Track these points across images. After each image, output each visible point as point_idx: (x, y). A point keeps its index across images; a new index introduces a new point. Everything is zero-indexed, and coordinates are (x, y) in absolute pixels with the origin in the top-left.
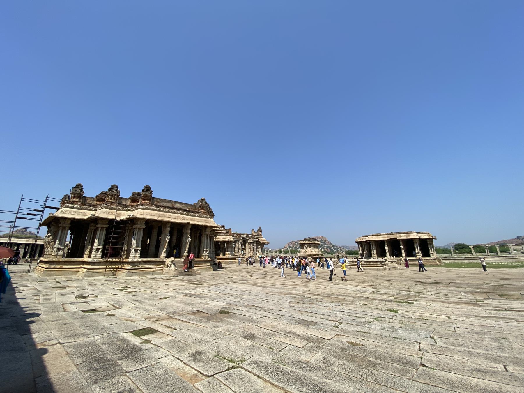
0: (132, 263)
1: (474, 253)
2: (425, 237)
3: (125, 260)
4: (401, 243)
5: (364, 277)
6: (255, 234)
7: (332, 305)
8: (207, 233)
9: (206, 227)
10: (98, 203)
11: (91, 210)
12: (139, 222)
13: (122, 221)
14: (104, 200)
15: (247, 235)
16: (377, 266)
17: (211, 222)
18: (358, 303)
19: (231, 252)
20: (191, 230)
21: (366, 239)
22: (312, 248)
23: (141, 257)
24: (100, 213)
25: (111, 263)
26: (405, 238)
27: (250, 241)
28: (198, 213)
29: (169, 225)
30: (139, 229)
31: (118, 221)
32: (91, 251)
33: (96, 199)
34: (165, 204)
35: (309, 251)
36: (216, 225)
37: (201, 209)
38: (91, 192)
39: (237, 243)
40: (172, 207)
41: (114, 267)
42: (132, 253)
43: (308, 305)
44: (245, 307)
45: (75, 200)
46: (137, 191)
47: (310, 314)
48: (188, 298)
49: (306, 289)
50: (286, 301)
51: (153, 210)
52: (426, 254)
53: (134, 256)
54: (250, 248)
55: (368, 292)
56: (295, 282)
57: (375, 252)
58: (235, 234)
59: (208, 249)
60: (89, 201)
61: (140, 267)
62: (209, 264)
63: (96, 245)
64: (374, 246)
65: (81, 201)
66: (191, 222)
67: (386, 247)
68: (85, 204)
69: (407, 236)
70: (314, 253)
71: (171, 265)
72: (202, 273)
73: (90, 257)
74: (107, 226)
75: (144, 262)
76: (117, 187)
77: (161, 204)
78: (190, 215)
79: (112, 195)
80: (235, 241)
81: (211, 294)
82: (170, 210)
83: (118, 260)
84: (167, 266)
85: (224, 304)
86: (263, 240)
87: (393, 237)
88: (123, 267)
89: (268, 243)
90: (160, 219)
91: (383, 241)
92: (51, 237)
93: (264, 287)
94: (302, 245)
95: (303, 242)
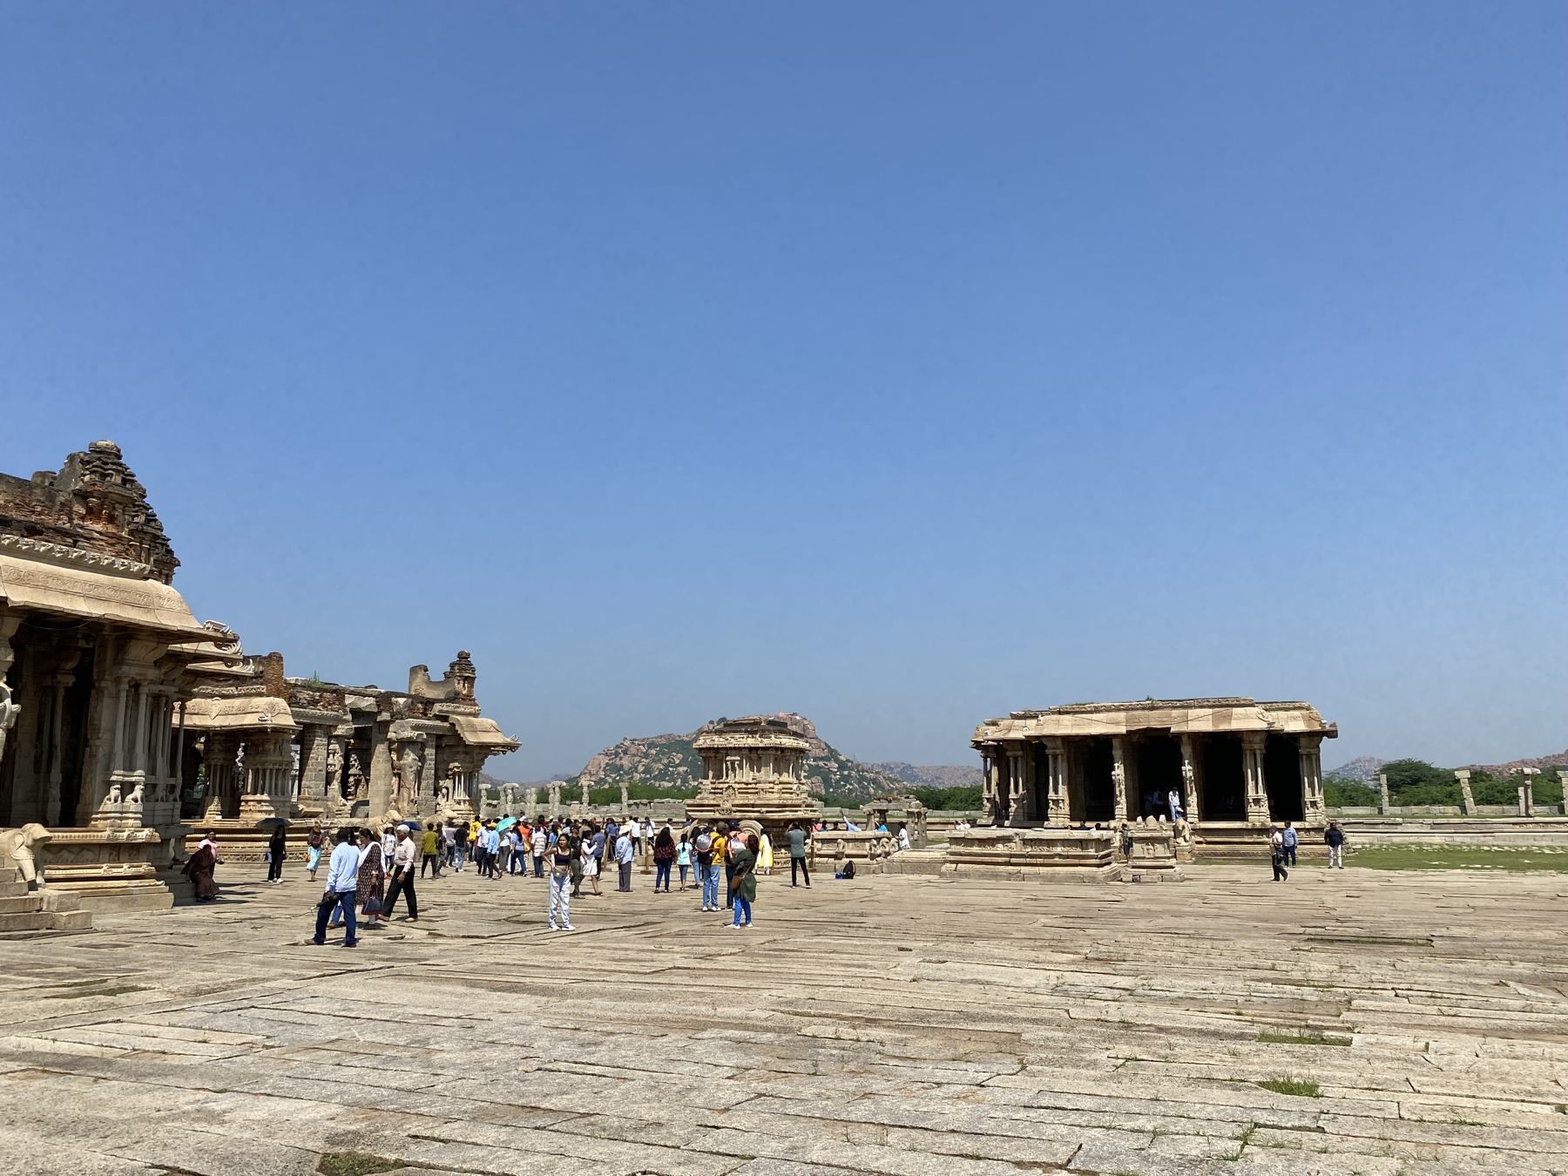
1: (1469, 802)
2: (1293, 724)
4: (1186, 750)
5: (1044, 920)
6: (430, 694)
7: (973, 1072)
8: (130, 671)
9: (126, 633)
15: (385, 700)
16: (1080, 861)
17: (164, 605)
18: (1102, 1056)
19: (279, 793)
21: (1029, 729)
22: (767, 774)
26: (1206, 726)
27: (403, 730)
28: (72, 537)
35: (746, 789)
36: (193, 625)
37: (92, 513)
39: (319, 742)
43: (851, 1085)
44: (478, 1117)
47: (894, 1136)
48: (51, 1083)
49: (793, 992)
50: (712, 1071)
52: (1287, 806)
54: (397, 772)
55: (1108, 994)
56: (708, 957)
57: (1063, 792)
58: (306, 686)
59: (138, 775)
62: (144, 867)
64: (1062, 766)
67: (1119, 772)
69: (1216, 719)
70: (774, 798)
72: (97, 922)
80: (305, 735)
81: (214, 1051)
85: (333, 1109)
86: (480, 728)
87: (1154, 720)
89: (512, 747)
91: (1104, 742)
93: (545, 991)
94: (714, 759)
95: (718, 741)
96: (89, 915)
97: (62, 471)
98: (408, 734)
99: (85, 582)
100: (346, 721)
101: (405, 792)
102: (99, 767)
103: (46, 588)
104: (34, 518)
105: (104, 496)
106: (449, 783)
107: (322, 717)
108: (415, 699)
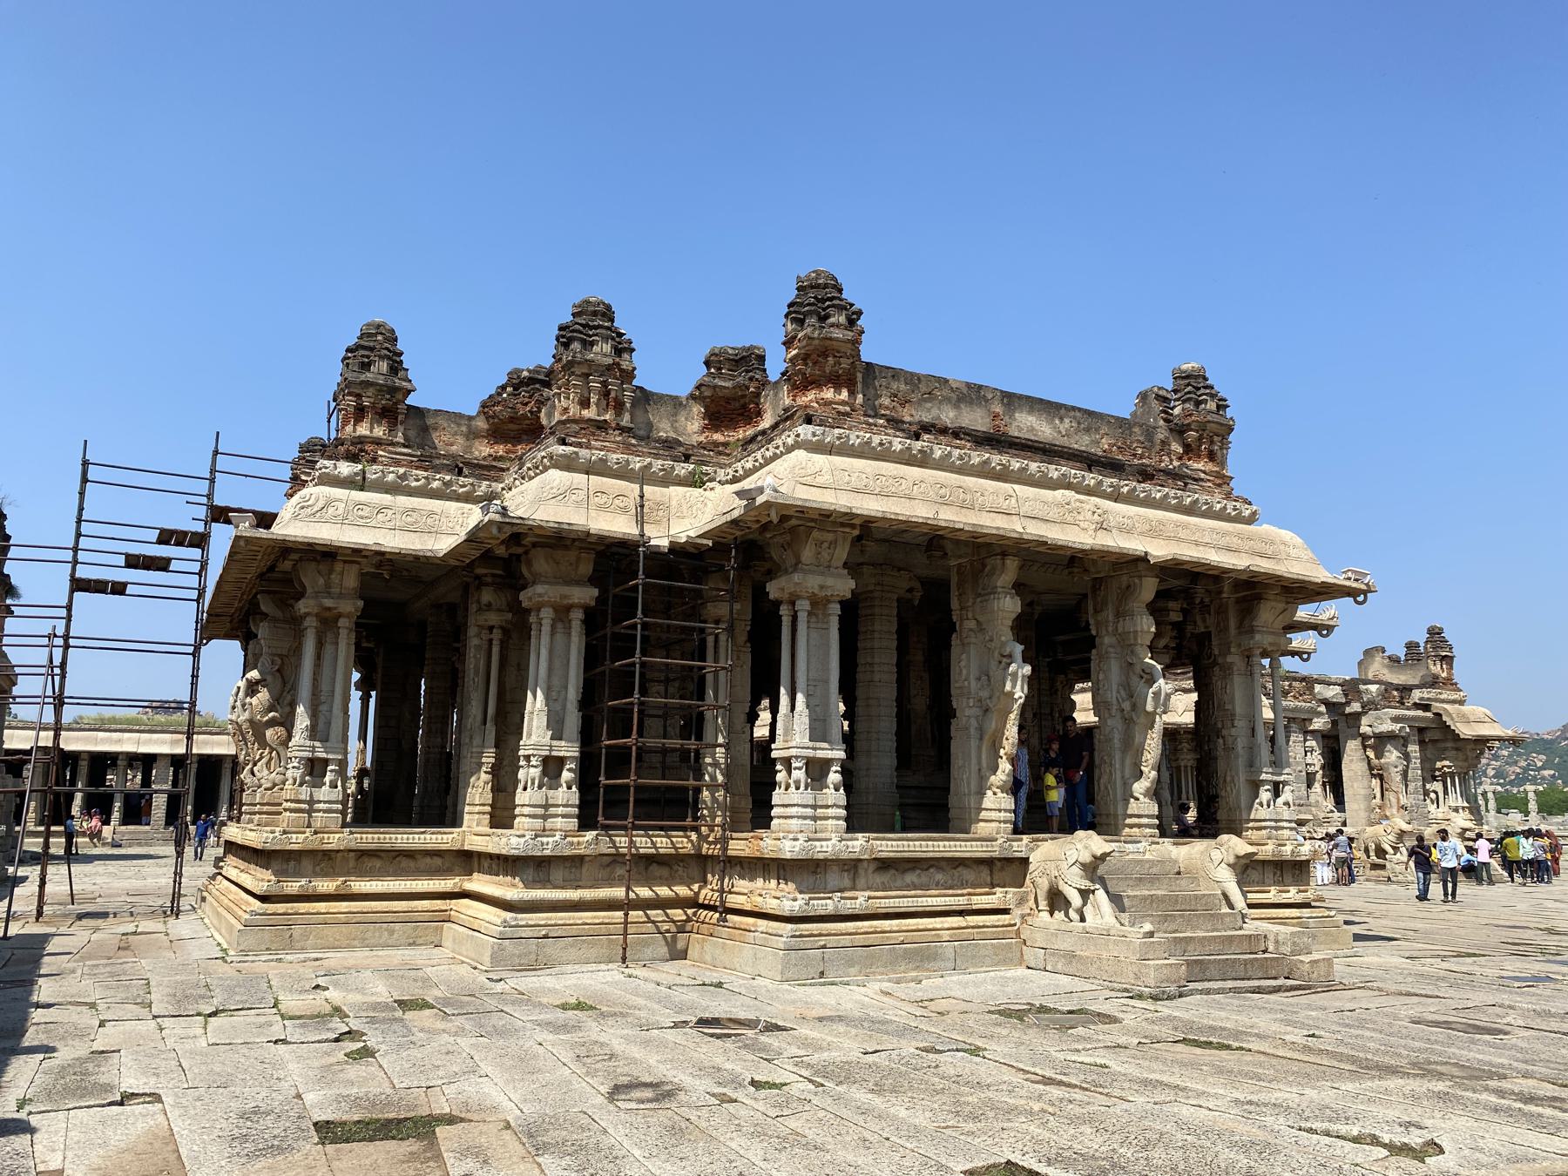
0: (805, 871)
3: (740, 846)
10: (500, 450)
11: (468, 498)
12: (807, 554)
13: (678, 551)
14: (532, 432)
15: (1351, 688)
20: (1154, 609)
23: (855, 822)
24: (539, 501)
25: (649, 867)
27: (1381, 722)
28: (1178, 477)
29: (1008, 573)
30: (818, 604)
31: (655, 555)
32: (504, 786)
33: (481, 424)
34: (948, 416)
36: (1321, 575)
38: (451, 378)
39: (1296, 737)
40: (998, 435)
41: (664, 891)
42: (789, 796)
45: (363, 430)
46: (735, 339)
51: (884, 455)
53: (808, 819)
60: (448, 442)
61: (860, 901)
63: (536, 733)
65: (400, 438)
66: (1159, 551)
68: (428, 460)
71: (1085, 894)
73: (501, 816)
74: (588, 595)
75: (885, 865)
76: (608, 313)
77: (926, 417)
78: (1130, 499)
79: (590, 369)
82: (997, 459)
83: (684, 843)
84: (1057, 900)
86: (1472, 718)
88: (734, 901)
90: (949, 516)
92: (263, 695)
96: (1329, 961)
97: (1134, 414)
98: (1387, 727)
99: (1213, 530)
100: (1320, 714)
101: (1390, 796)
102: (1241, 762)
103: (1180, 540)
104: (1136, 462)
105: (1202, 427)
106: (1438, 786)
107: (1296, 709)
108: (1389, 687)
